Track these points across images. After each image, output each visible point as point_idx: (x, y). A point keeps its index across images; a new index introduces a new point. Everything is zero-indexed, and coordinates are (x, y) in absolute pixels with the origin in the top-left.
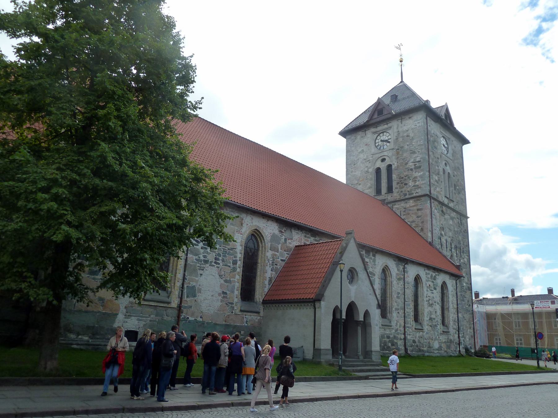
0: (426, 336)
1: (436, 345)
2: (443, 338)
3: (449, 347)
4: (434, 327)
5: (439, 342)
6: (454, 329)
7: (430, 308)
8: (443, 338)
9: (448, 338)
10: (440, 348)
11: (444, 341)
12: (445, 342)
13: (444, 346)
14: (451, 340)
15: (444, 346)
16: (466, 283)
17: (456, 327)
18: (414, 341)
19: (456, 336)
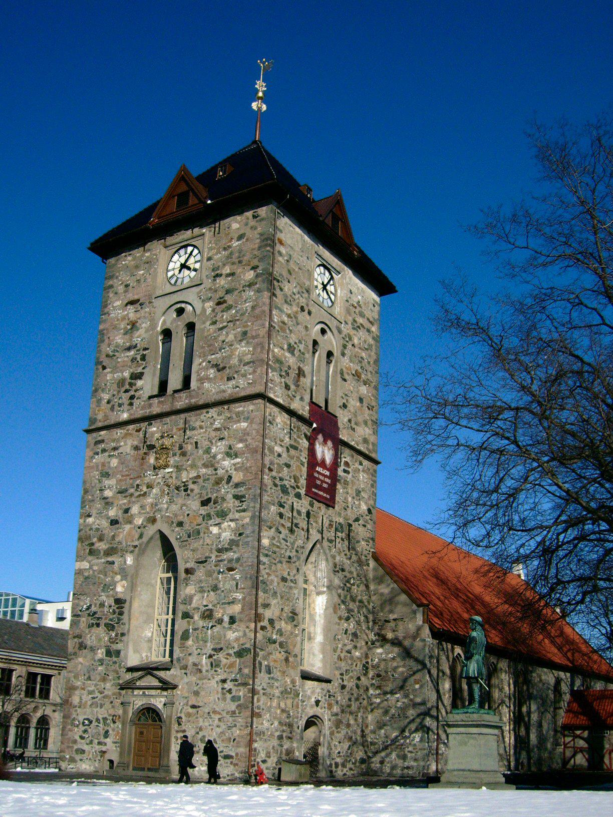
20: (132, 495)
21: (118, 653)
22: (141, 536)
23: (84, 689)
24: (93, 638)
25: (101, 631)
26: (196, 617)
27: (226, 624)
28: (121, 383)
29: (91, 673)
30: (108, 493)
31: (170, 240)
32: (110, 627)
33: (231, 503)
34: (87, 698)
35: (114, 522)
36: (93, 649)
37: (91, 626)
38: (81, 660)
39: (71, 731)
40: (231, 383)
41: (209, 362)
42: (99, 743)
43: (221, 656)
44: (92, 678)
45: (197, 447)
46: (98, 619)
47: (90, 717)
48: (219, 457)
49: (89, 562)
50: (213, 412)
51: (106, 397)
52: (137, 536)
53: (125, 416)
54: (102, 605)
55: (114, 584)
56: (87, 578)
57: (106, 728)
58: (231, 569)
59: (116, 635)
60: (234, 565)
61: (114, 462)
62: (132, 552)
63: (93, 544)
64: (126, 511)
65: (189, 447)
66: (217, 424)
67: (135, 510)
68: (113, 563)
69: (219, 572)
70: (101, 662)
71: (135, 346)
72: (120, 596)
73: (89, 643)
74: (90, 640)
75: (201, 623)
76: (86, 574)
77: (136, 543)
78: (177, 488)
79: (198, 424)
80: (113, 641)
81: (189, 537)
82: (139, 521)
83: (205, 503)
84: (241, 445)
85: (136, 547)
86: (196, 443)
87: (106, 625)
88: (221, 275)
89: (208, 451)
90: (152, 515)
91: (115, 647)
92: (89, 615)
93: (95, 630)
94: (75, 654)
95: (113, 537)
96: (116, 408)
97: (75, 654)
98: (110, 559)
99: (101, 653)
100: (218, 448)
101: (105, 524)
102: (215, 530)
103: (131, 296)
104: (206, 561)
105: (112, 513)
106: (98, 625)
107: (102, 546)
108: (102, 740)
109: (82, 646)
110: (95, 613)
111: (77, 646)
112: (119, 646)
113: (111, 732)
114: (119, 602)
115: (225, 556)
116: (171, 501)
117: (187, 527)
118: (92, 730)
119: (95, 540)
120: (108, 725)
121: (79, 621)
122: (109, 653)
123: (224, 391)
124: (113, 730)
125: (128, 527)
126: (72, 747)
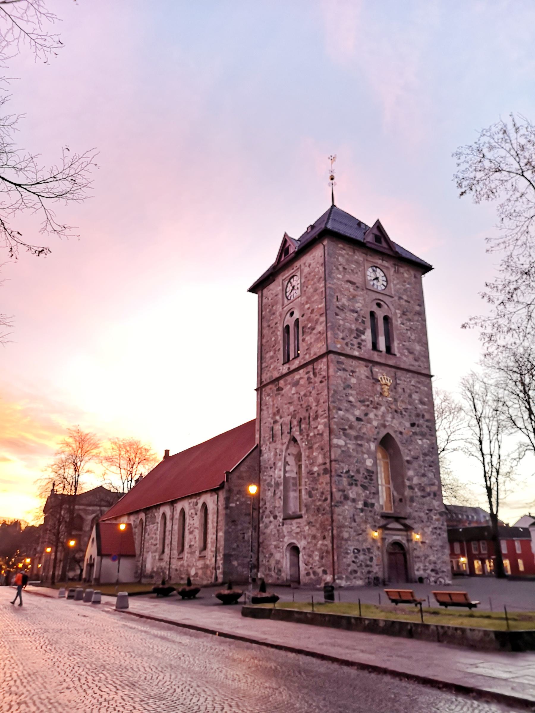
0: (185, 564)
1: (193, 572)
2: (200, 564)
3: (205, 573)
4: (192, 553)
5: (196, 569)
6: (212, 552)
7: (191, 536)
8: (200, 564)
9: (205, 564)
10: (196, 574)
11: (200, 566)
12: (201, 568)
13: (200, 572)
14: (207, 565)
15: (200, 572)
16: (319, 466)
17: (214, 549)
18: (176, 570)
19: (214, 559)
20: (368, 406)
21: (373, 505)
22: (378, 433)
23: (351, 528)
24: (354, 493)
25: (359, 490)
26: (416, 490)
27: (432, 496)
28: (351, 331)
29: (356, 517)
30: (351, 398)
31: (369, 258)
32: (364, 487)
33: (425, 430)
34: (353, 534)
35: (359, 419)
36: (354, 500)
37: (351, 484)
38: (346, 507)
39: (345, 558)
40: (416, 364)
41: (403, 345)
42: (367, 566)
43: (432, 514)
44: (357, 520)
45: (404, 391)
46: (356, 480)
47: (358, 547)
48: (417, 401)
49: (345, 441)
50: (409, 375)
51: (341, 335)
52: (376, 433)
53: (356, 353)
54: (358, 471)
55: (365, 460)
56: (343, 451)
57: (371, 555)
58: (430, 466)
59: (370, 493)
60: (432, 464)
61: (354, 381)
62: (373, 442)
63: (345, 430)
64: (366, 415)
65: (400, 390)
66: (413, 383)
67: (371, 416)
68: (361, 445)
69: (425, 467)
70: (362, 510)
71: (357, 312)
72: (369, 468)
73: (351, 496)
74: (352, 495)
75: (419, 494)
76: (343, 449)
77: (375, 437)
78: (396, 411)
79: (402, 378)
80: (367, 497)
81: (406, 441)
82: (375, 423)
83: (413, 425)
84: (426, 399)
85: (375, 439)
86: (403, 389)
87: (362, 486)
88: (402, 299)
89: (410, 396)
90: (382, 422)
91: (370, 501)
92: (348, 477)
93: (354, 487)
94: (341, 502)
95: (360, 429)
96: (350, 345)
97: (341, 502)
98: (359, 442)
99: (360, 505)
100: (415, 396)
101: (352, 419)
102: (420, 442)
103: (348, 277)
104: (417, 458)
105: (357, 413)
106: (356, 485)
107: (353, 433)
108: (369, 563)
109: (346, 498)
110: (353, 476)
111: (342, 498)
112: (373, 501)
113: (374, 558)
114: (368, 471)
115: (428, 458)
116: (393, 418)
117: (405, 436)
118: (361, 557)
119: (347, 427)
120: (372, 553)
121: (342, 480)
122: (366, 504)
123: (413, 366)
124: (375, 556)
125: (369, 425)
126: (347, 570)
